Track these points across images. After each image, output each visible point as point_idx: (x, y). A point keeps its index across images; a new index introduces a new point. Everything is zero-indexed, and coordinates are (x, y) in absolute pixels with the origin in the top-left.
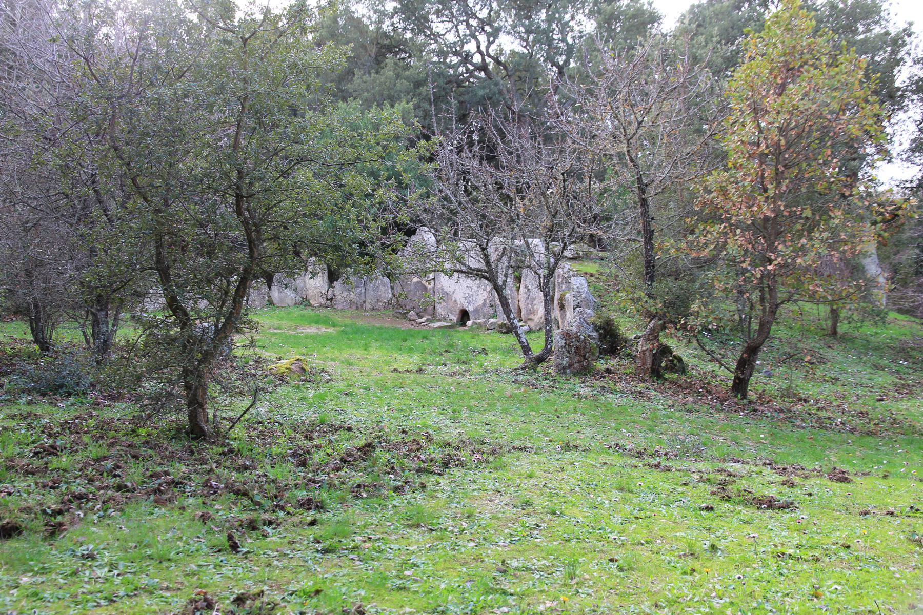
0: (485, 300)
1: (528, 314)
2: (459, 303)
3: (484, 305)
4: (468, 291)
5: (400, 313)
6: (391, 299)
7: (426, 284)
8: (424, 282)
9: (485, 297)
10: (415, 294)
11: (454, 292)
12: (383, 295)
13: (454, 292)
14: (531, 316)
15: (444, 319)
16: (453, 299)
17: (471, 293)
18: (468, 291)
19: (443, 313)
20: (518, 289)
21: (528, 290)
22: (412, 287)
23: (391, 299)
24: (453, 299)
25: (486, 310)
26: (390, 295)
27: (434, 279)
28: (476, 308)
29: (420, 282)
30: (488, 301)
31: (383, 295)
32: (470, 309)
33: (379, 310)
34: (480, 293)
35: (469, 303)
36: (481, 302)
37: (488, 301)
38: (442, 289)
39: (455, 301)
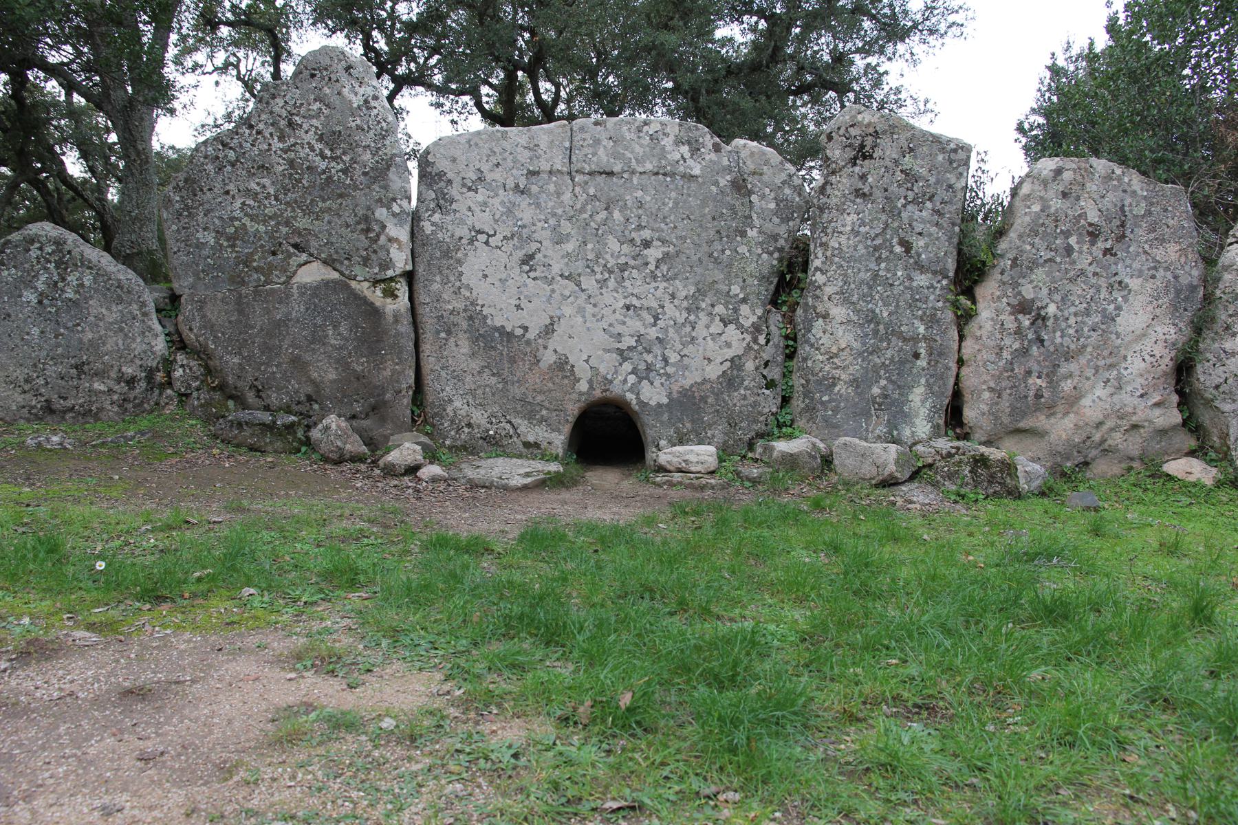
0: (736, 363)
1: (1018, 412)
2: (583, 372)
3: (731, 380)
4: (634, 325)
5: (270, 427)
6: (168, 364)
7: (376, 296)
8: (364, 288)
9: (737, 349)
10: (317, 338)
11: (549, 330)
12: (113, 342)
13: (549, 330)
14: (1039, 421)
15: (495, 445)
16: (548, 358)
17: (653, 333)
18: (634, 325)
19: (479, 417)
20: (964, 318)
21: (1040, 319)
22: (297, 308)
23: (168, 364)
24: (548, 358)
25: (737, 400)
26: (160, 345)
27: (410, 277)
28: (684, 393)
29: (341, 286)
30: (750, 365)
31: (113, 342)
32: (653, 394)
33: (88, 414)
34: (700, 331)
35: (646, 373)
36: (714, 372)
37: (750, 365)
38: (474, 316)
39: (563, 366)
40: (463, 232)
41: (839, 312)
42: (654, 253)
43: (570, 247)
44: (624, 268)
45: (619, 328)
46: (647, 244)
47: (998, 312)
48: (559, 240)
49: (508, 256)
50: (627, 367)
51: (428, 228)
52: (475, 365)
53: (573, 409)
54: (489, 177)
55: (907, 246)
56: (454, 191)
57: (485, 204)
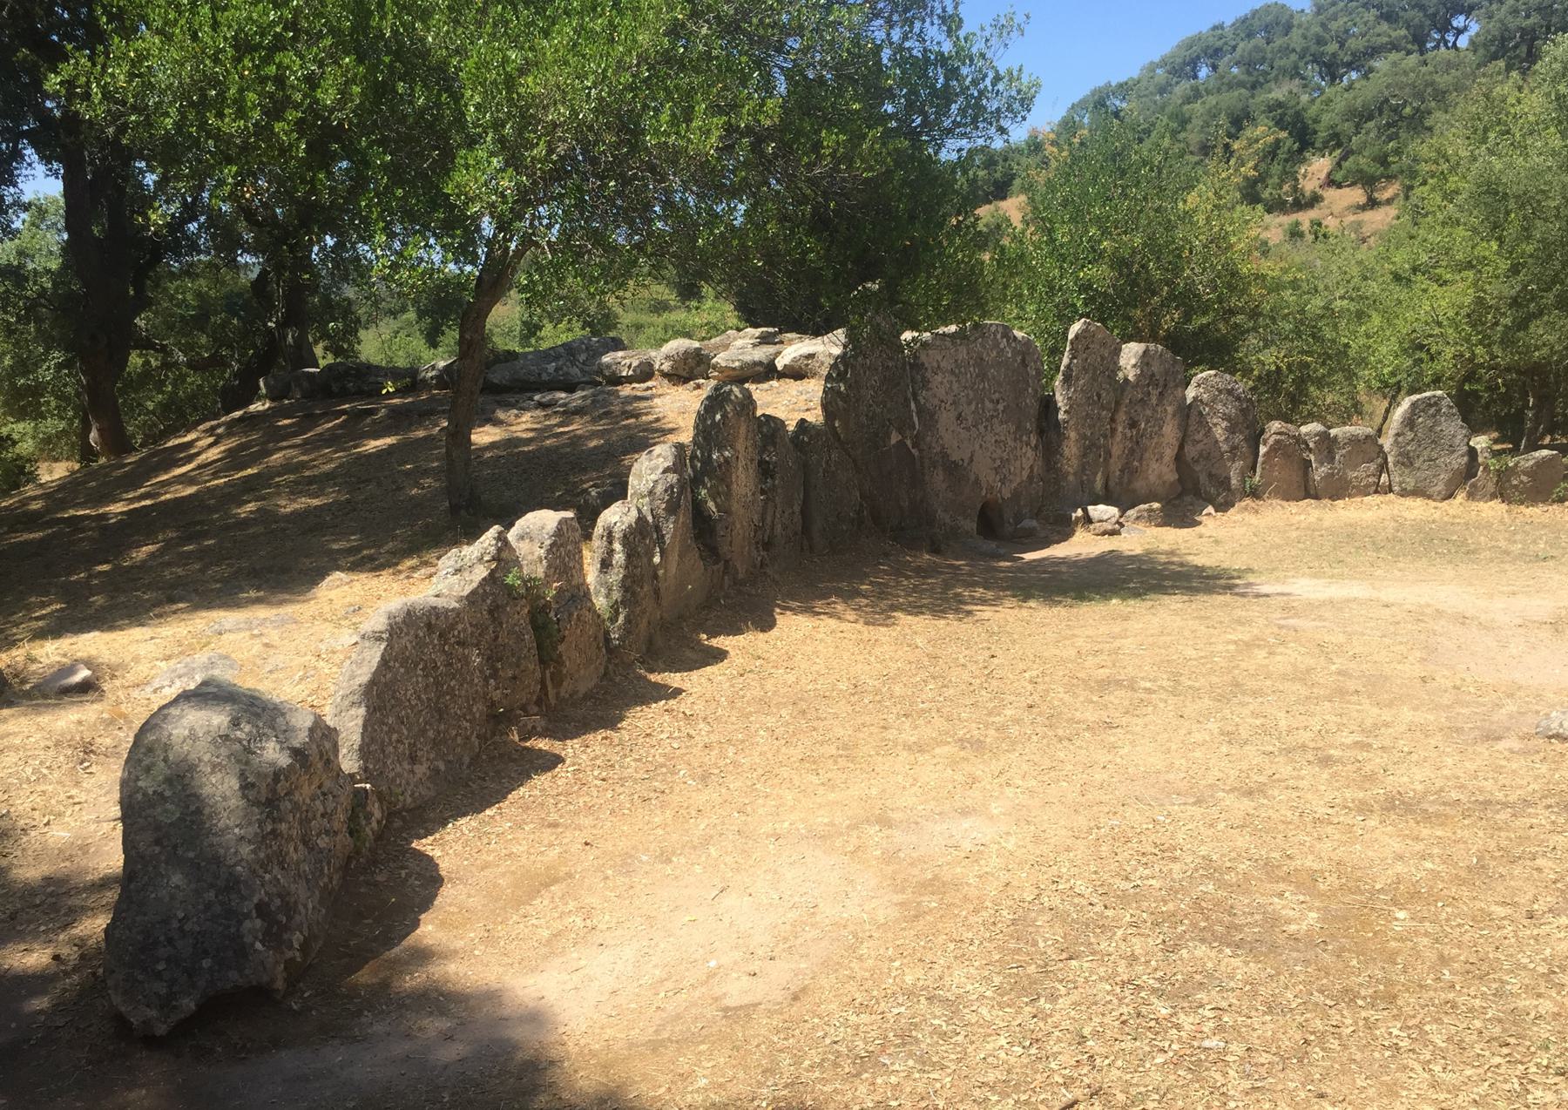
0: (1031, 467)
2: (984, 485)
16: (972, 478)
24: (972, 478)
36: (1025, 474)
38: (945, 455)
39: (977, 481)
40: (936, 402)
41: (1073, 435)
42: (1000, 407)
43: (973, 407)
44: (992, 416)
45: (994, 456)
46: (998, 402)
47: (1124, 428)
48: (969, 404)
49: (953, 415)
50: (998, 477)
51: (922, 401)
52: (944, 486)
53: (979, 506)
54: (942, 365)
55: (1099, 396)
56: (928, 374)
57: (942, 383)
